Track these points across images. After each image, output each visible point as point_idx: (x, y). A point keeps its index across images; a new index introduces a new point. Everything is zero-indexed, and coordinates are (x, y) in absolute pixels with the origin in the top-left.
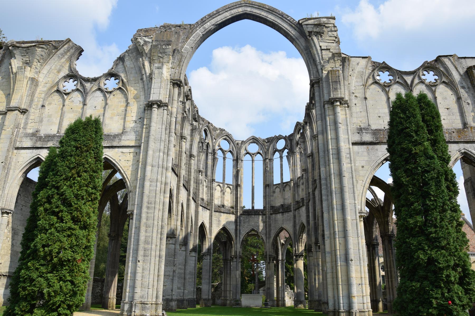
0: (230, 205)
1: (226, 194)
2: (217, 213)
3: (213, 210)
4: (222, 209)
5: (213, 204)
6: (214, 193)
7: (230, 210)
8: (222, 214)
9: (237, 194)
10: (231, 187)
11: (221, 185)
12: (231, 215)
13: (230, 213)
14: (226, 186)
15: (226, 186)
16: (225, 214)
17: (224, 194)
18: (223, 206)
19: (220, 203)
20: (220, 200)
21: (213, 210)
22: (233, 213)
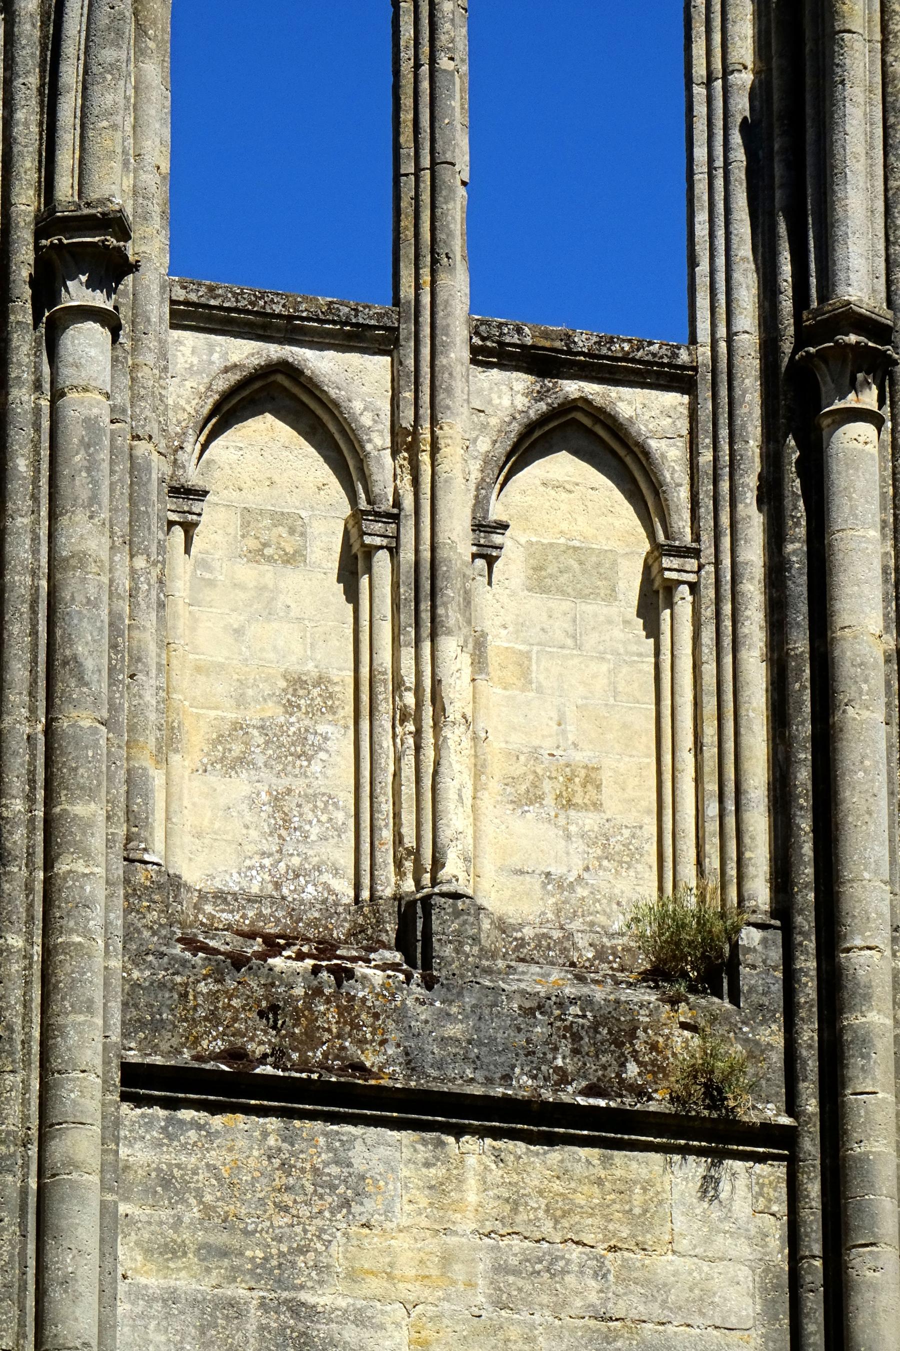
0: (624, 896)
1: (500, 604)
2: (243, 1140)
3: (93, 1042)
4: (405, 1027)
5: (91, 871)
6: (86, 590)
7: (616, 1032)
8: (385, 1153)
9: (804, 594)
10: (653, 415)
11: (358, 381)
12: (676, 1178)
13: (615, 1128)
14: (510, 395)
15: (510, 395)
16: (473, 1152)
17: (425, 602)
18: (417, 928)
19: (328, 872)
20: (334, 769)
21: (93, 1042)
22: (707, 1129)
